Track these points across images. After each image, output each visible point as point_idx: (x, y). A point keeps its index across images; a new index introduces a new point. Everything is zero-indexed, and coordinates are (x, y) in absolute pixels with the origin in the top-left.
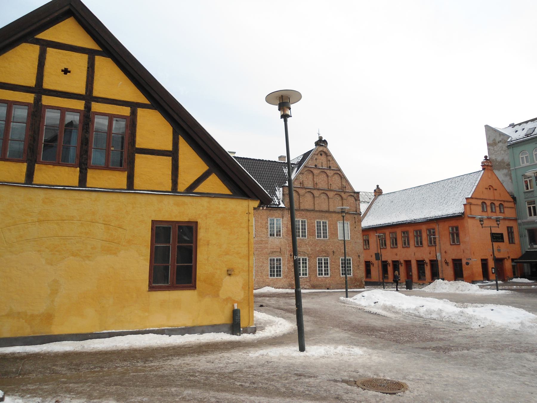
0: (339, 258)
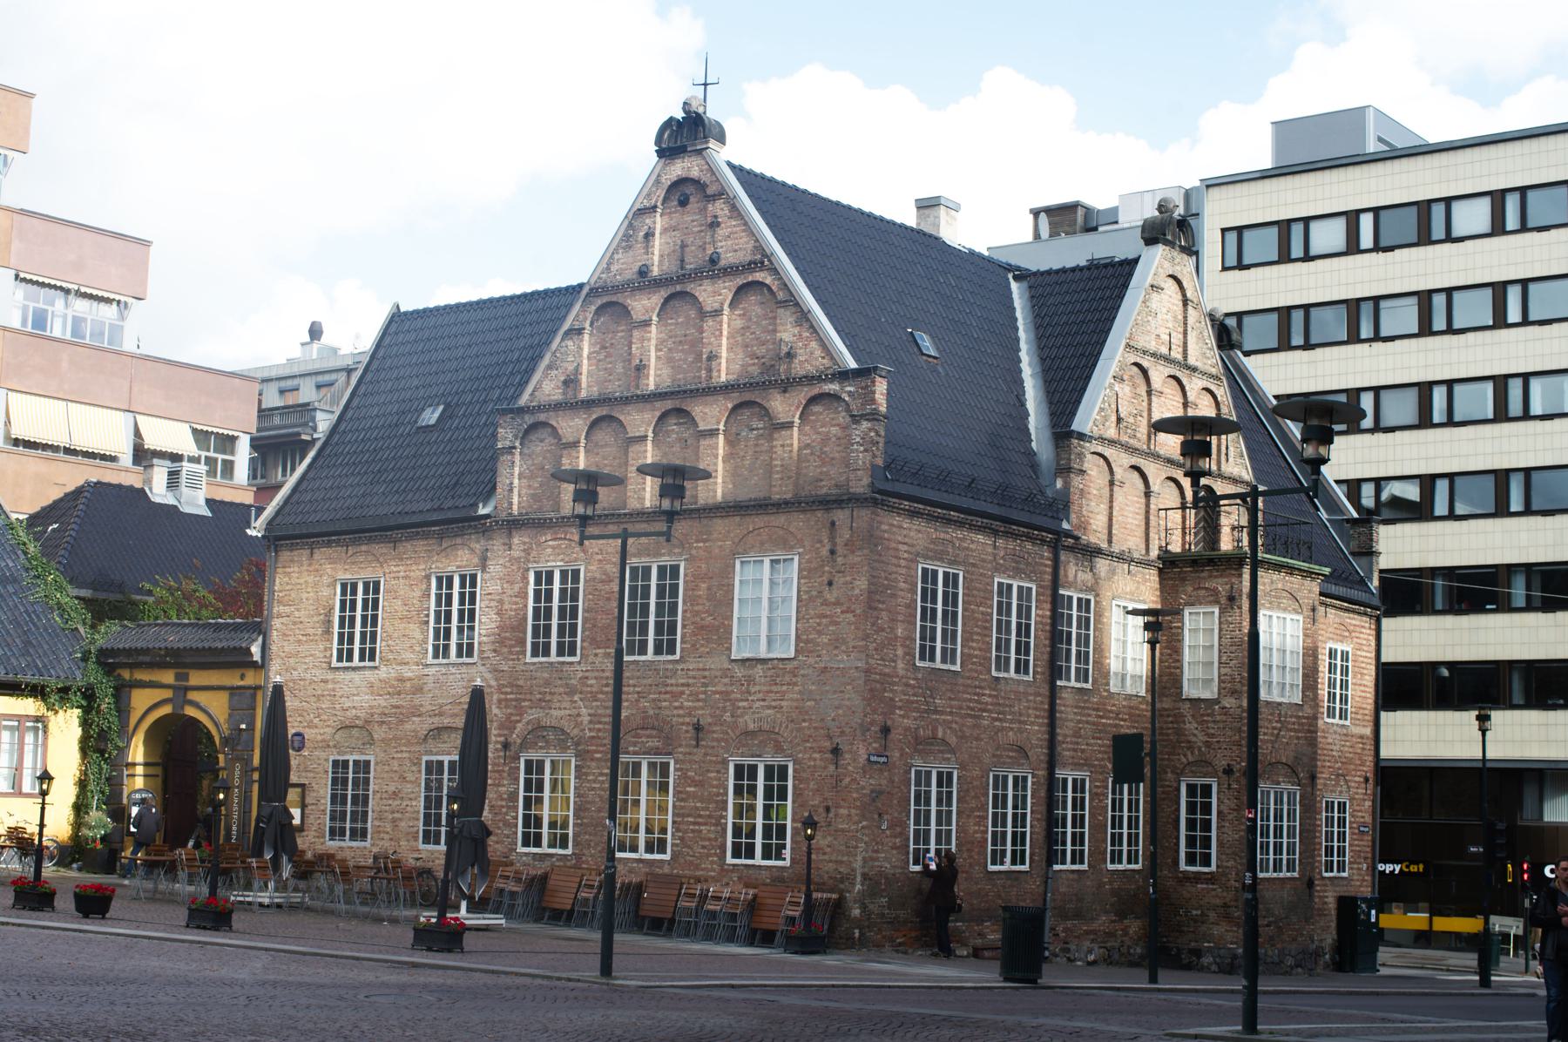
0: (725, 762)
